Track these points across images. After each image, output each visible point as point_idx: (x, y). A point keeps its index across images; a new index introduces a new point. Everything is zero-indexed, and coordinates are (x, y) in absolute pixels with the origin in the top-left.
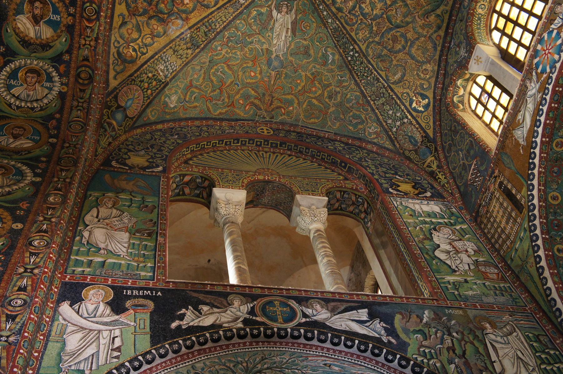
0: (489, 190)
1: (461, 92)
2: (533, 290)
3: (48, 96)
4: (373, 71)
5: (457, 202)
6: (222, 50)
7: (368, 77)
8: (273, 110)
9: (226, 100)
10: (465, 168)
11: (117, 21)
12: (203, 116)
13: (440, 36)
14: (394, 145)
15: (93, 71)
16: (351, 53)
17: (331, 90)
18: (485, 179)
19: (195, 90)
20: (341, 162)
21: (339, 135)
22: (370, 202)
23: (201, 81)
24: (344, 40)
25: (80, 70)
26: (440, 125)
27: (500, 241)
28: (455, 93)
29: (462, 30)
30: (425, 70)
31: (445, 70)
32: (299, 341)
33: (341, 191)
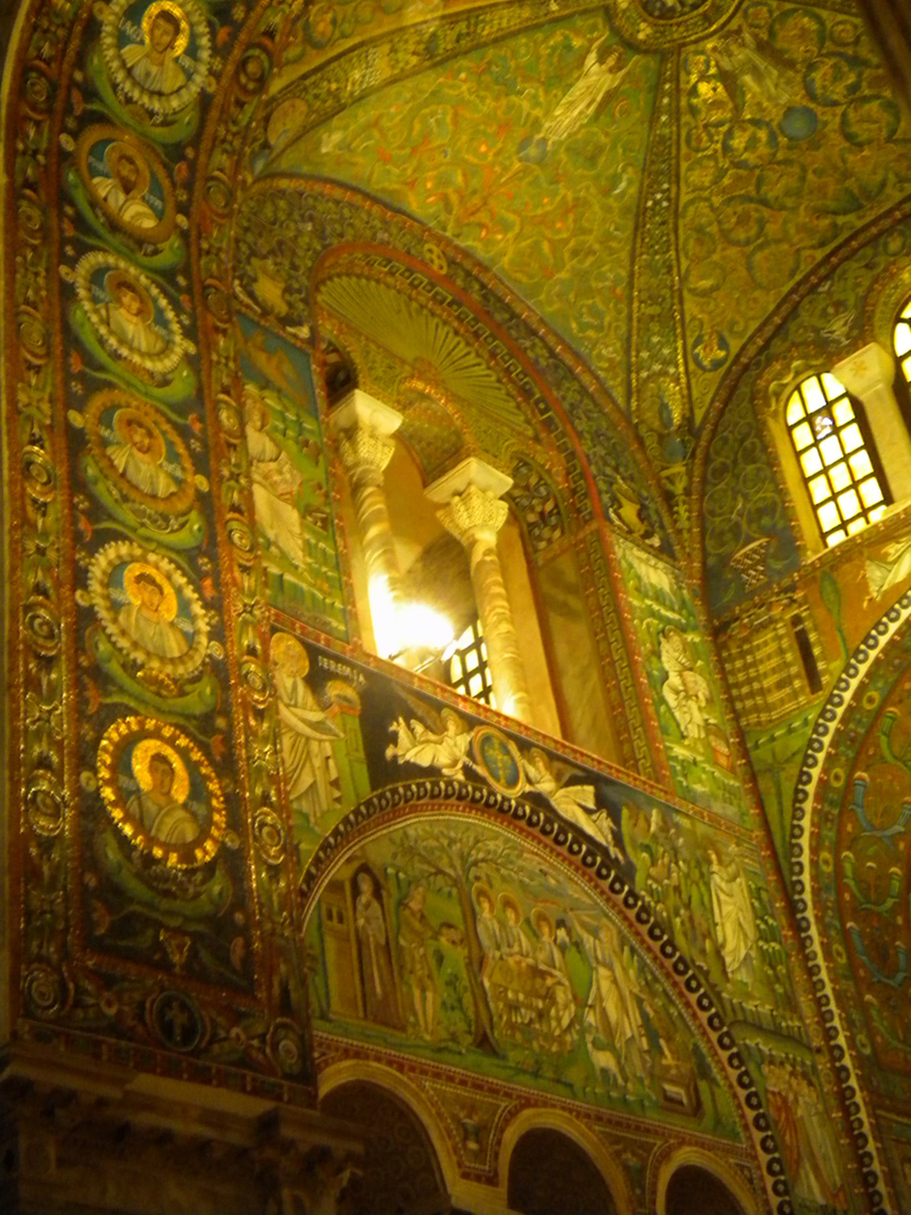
0: (769, 610)
1: (788, 379)
3: (183, 91)
5: (691, 577)
7: (656, 253)
8: (468, 225)
9: (409, 172)
12: (354, 183)
13: (813, 258)
15: (271, 66)
16: (659, 196)
18: (768, 585)
19: (376, 134)
26: (722, 413)
28: (780, 376)
29: (858, 285)
30: (755, 300)
31: (785, 320)
32: (517, 822)
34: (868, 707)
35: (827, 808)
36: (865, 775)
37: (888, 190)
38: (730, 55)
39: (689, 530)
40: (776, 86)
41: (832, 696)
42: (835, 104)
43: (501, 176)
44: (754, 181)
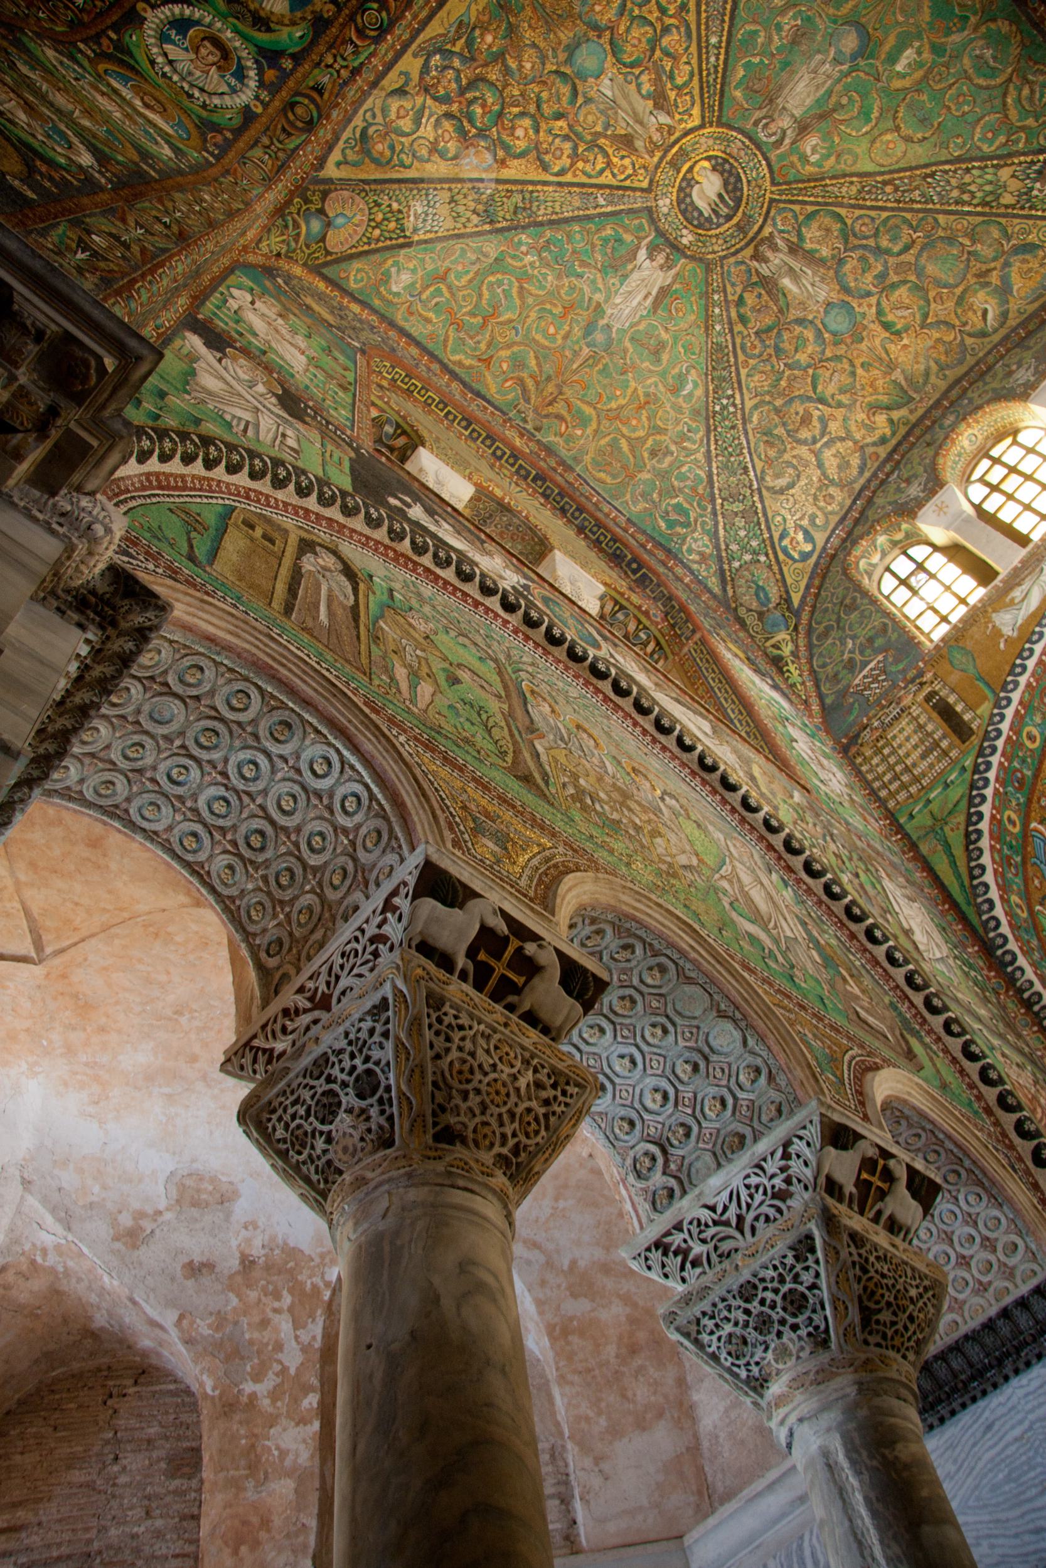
1: (876, 559)
2: (942, 867)
4: (745, 451)
5: (811, 716)
6: (526, 254)
8: (547, 416)
9: (483, 346)
10: (851, 666)
11: (392, 80)
12: (430, 346)
13: (878, 456)
14: (724, 590)
15: (320, 117)
16: (725, 402)
17: (661, 442)
18: (894, 686)
20: (634, 560)
21: (634, 525)
22: (662, 642)
23: (464, 281)
24: (724, 373)
25: (298, 99)
26: (817, 595)
27: (893, 787)
30: (832, 497)
31: (862, 513)
32: (600, 684)
33: (616, 602)
34: (1028, 744)
35: (1006, 851)
36: (1040, 827)
37: (933, 379)
38: (766, 261)
39: (803, 683)
40: (813, 285)
41: (986, 732)
42: (869, 294)
43: (572, 361)
44: (809, 380)
